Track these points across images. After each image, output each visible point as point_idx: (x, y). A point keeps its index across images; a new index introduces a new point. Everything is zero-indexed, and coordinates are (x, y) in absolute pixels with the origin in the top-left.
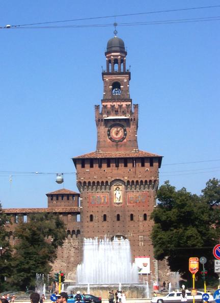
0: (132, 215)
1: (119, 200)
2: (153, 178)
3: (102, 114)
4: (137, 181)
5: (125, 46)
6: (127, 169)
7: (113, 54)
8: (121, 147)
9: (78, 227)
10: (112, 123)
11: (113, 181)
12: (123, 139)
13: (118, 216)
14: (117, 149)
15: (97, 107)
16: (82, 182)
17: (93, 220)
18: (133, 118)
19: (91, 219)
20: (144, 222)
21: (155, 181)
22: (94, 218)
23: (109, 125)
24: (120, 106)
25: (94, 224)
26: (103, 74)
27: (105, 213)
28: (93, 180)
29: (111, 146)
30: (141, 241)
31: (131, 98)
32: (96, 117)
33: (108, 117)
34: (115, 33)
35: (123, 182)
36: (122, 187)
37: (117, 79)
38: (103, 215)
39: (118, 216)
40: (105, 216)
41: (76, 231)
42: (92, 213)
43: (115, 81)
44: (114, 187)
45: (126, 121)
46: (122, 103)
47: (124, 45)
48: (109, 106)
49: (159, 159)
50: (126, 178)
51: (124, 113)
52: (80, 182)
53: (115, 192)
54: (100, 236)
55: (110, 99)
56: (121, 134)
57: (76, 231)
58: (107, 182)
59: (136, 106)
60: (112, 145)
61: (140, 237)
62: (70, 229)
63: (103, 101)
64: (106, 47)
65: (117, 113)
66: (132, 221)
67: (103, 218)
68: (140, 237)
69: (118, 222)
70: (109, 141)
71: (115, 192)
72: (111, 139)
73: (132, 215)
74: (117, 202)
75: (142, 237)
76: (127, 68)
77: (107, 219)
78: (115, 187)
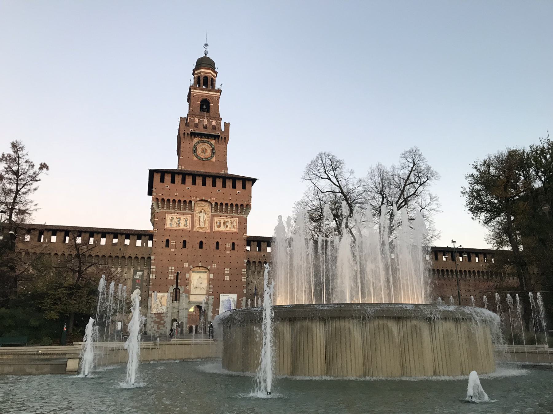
0: (217, 243)
1: (205, 225)
2: (245, 203)
4: (227, 204)
6: (216, 189)
7: (203, 70)
12: (211, 157)
13: (201, 243)
18: (223, 138)
20: (232, 251)
21: (247, 205)
23: (196, 140)
27: (185, 239)
30: (227, 275)
31: (220, 117)
34: (206, 52)
35: (210, 202)
36: (208, 209)
37: (205, 96)
39: (201, 243)
40: (185, 242)
41: (146, 258)
42: (168, 238)
43: (204, 97)
44: (197, 209)
45: (215, 139)
49: (253, 181)
52: (157, 199)
53: (198, 215)
55: (197, 115)
56: (209, 153)
59: (227, 125)
61: (226, 269)
62: (137, 256)
66: (218, 251)
67: (182, 243)
70: (194, 158)
71: (198, 215)
72: (197, 156)
73: (217, 243)
74: (202, 226)
75: (228, 269)
76: (217, 86)
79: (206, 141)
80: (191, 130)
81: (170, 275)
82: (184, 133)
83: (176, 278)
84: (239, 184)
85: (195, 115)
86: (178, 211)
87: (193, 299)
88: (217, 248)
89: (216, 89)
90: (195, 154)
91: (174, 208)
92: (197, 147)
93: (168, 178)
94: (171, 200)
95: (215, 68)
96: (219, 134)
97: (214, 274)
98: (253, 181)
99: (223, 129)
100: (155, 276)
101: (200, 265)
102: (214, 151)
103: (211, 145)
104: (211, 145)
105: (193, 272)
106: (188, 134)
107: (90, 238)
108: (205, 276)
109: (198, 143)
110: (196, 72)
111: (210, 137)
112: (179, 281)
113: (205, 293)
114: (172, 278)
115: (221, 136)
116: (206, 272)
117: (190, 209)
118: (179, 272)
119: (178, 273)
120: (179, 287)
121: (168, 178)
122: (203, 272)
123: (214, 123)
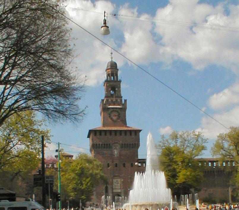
2: (137, 142)
11: (113, 144)
16: (95, 144)
23: (110, 111)
31: (122, 96)
33: (109, 106)
34: (112, 58)
38: (107, 164)
46: (117, 99)
48: (110, 100)
49: (140, 131)
50: (121, 142)
51: (119, 105)
52: (94, 144)
58: (110, 144)
59: (125, 101)
61: (129, 176)
63: (106, 97)
68: (129, 176)
70: (110, 120)
72: (112, 119)
84: (133, 134)
87: (114, 191)
88: (124, 166)
89: (119, 80)
93: (98, 134)
98: (140, 131)
99: (123, 102)
101: (116, 175)
104: (118, 112)
108: (119, 180)
109: (112, 112)
110: (107, 71)
113: (119, 188)
116: (119, 178)
120: (108, 186)
121: (98, 134)
123: (119, 100)
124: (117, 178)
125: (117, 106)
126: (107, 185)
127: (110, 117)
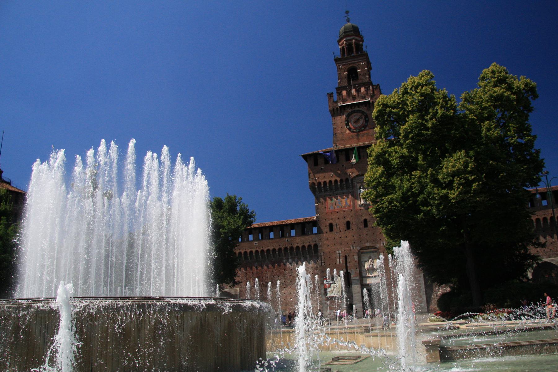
3: (337, 102)
5: (360, 30)
8: (363, 136)
9: (314, 240)
10: (350, 110)
13: (365, 221)
14: (358, 139)
15: (331, 95)
17: (334, 230)
19: (331, 229)
22: (335, 227)
23: (346, 113)
24: (358, 91)
25: (335, 234)
26: (336, 60)
27: (348, 219)
28: (330, 179)
29: (351, 137)
32: (329, 107)
38: (345, 222)
39: (365, 221)
41: (312, 246)
42: (331, 221)
45: (366, 106)
47: (358, 30)
51: (364, 98)
52: (314, 184)
54: (343, 249)
57: (312, 246)
60: (352, 137)
64: (338, 35)
65: (354, 98)
67: (345, 225)
69: (366, 229)
70: (348, 131)
77: (352, 226)
78: (359, 185)
79: (357, 110)
80: (341, 104)
81: (338, 260)
82: (334, 109)
83: (344, 262)
85: (344, 88)
86: (336, 192)
90: (348, 127)
91: (331, 189)
92: (349, 120)
94: (328, 181)
95: (359, 32)
96: (369, 99)
97: (383, 252)
100: (324, 262)
101: (368, 244)
102: (367, 119)
103: (363, 113)
105: (362, 253)
106: (337, 108)
107: (313, 228)
111: (360, 106)
112: (348, 265)
114: (341, 263)
115: (371, 102)
116: (376, 252)
117: (348, 187)
118: (347, 256)
119: (346, 257)
120: (349, 271)
122: (373, 252)
124: (370, 252)
125: (359, 101)
126: (347, 270)
127: (347, 125)
